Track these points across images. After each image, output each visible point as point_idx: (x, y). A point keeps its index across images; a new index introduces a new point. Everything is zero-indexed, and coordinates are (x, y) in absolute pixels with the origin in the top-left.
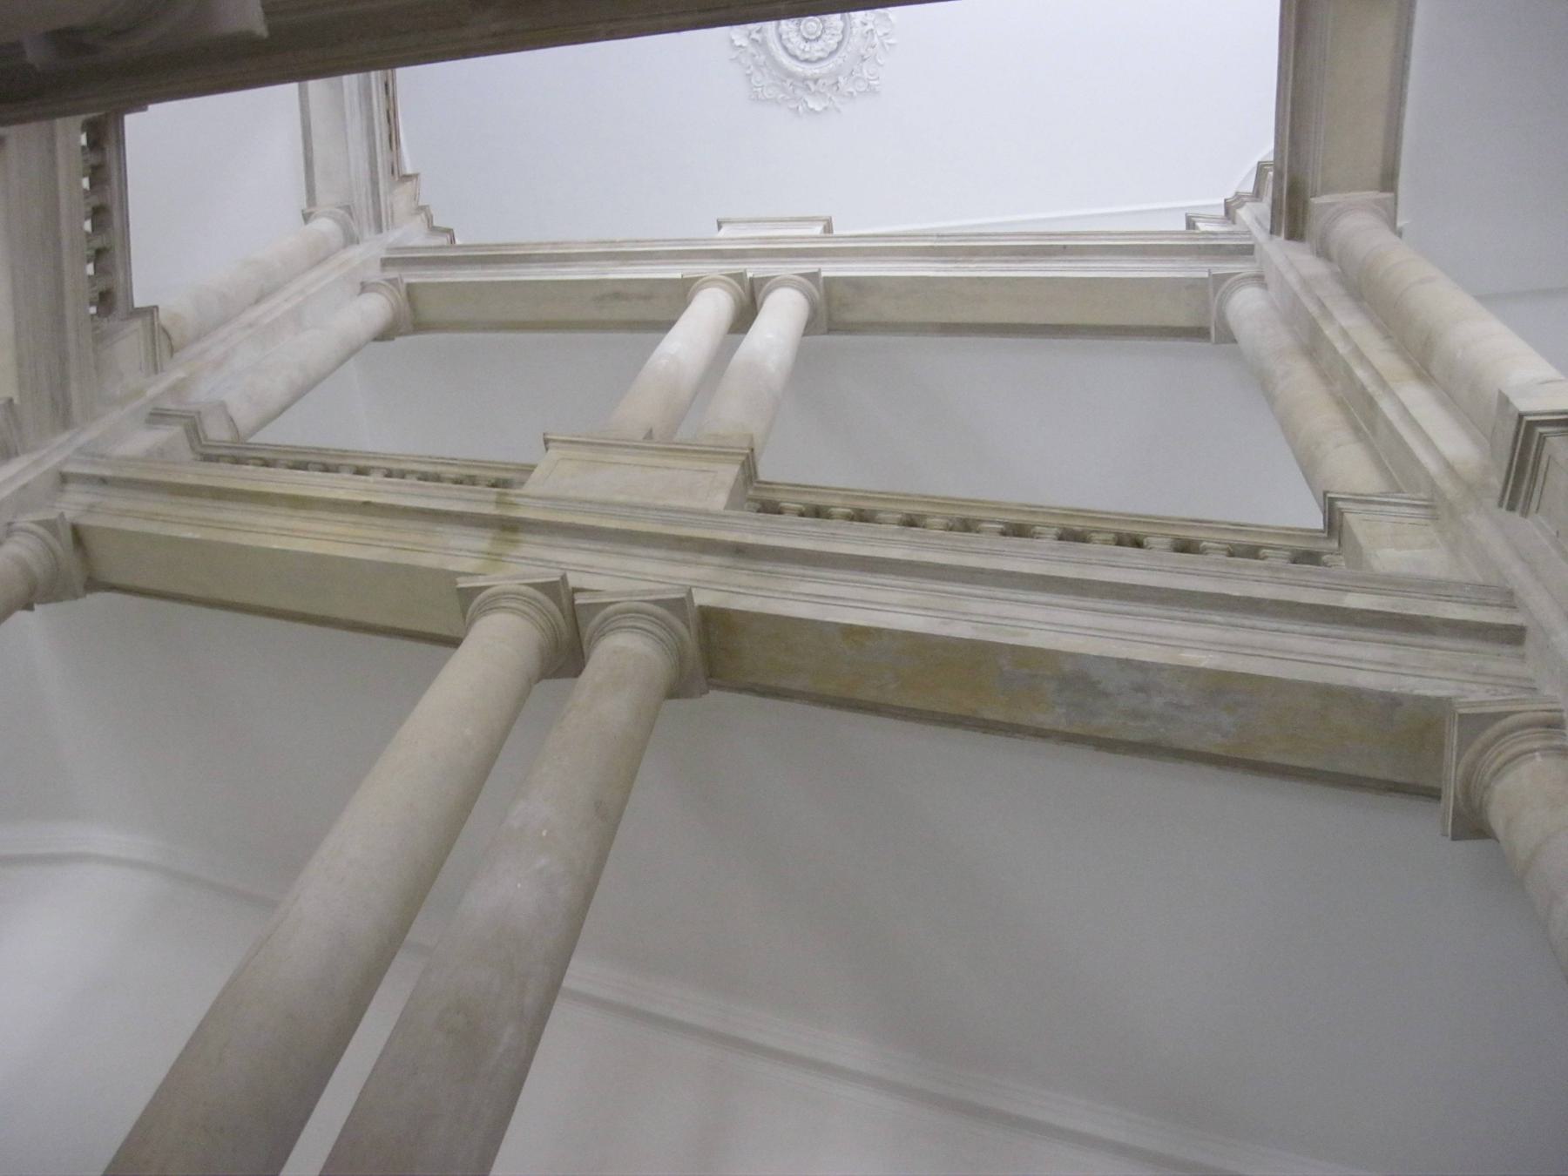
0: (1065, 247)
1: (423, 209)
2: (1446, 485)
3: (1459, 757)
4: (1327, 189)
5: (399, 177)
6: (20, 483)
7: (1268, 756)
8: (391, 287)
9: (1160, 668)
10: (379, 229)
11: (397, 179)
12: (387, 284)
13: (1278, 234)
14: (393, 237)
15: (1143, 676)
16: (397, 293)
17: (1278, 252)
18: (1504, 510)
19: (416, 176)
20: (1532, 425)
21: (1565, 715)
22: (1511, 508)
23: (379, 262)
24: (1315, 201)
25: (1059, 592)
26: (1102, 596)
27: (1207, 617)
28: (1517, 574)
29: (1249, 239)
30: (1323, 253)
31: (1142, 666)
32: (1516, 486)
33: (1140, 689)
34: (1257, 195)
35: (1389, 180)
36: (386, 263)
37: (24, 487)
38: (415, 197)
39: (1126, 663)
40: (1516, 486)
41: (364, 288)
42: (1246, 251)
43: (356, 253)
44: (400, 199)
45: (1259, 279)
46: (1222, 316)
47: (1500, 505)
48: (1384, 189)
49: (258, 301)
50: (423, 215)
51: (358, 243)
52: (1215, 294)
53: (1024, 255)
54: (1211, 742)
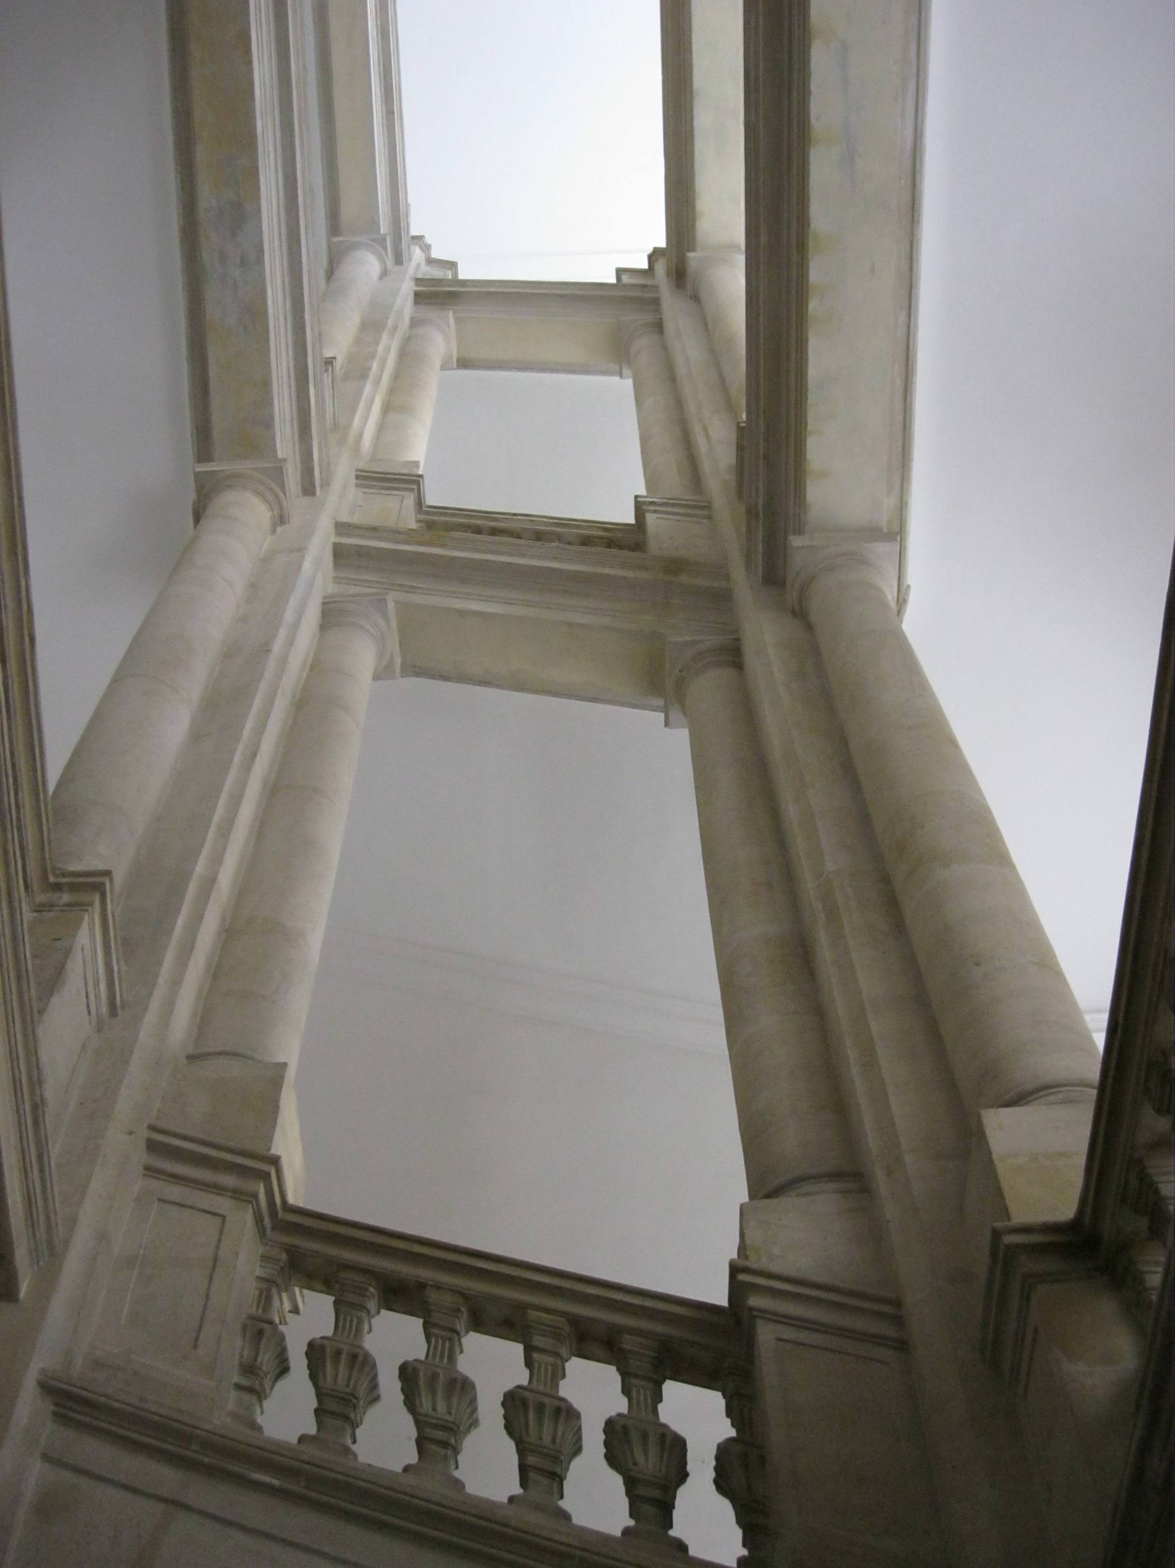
0: (393, 113)
2: (351, 438)
3: (254, 469)
4: (459, 321)
7: (212, 352)
9: (262, 273)
13: (417, 285)
15: (253, 261)
17: (407, 288)
18: (355, 473)
20: (418, 483)
21: (287, 525)
22: (357, 477)
24: (451, 312)
25: (286, 194)
26: (288, 223)
27: (288, 299)
28: (336, 486)
29: (406, 262)
30: (415, 323)
31: (260, 260)
32: (375, 479)
33: (243, 262)
34: (431, 261)
35: (464, 363)
39: (260, 251)
40: (375, 479)
42: (399, 260)
45: (384, 273)
46: (355, 246)
47: (357, 470)
48: (458, 360)
52: (373, 240)
53: (385, 77)
54: (212, 311)
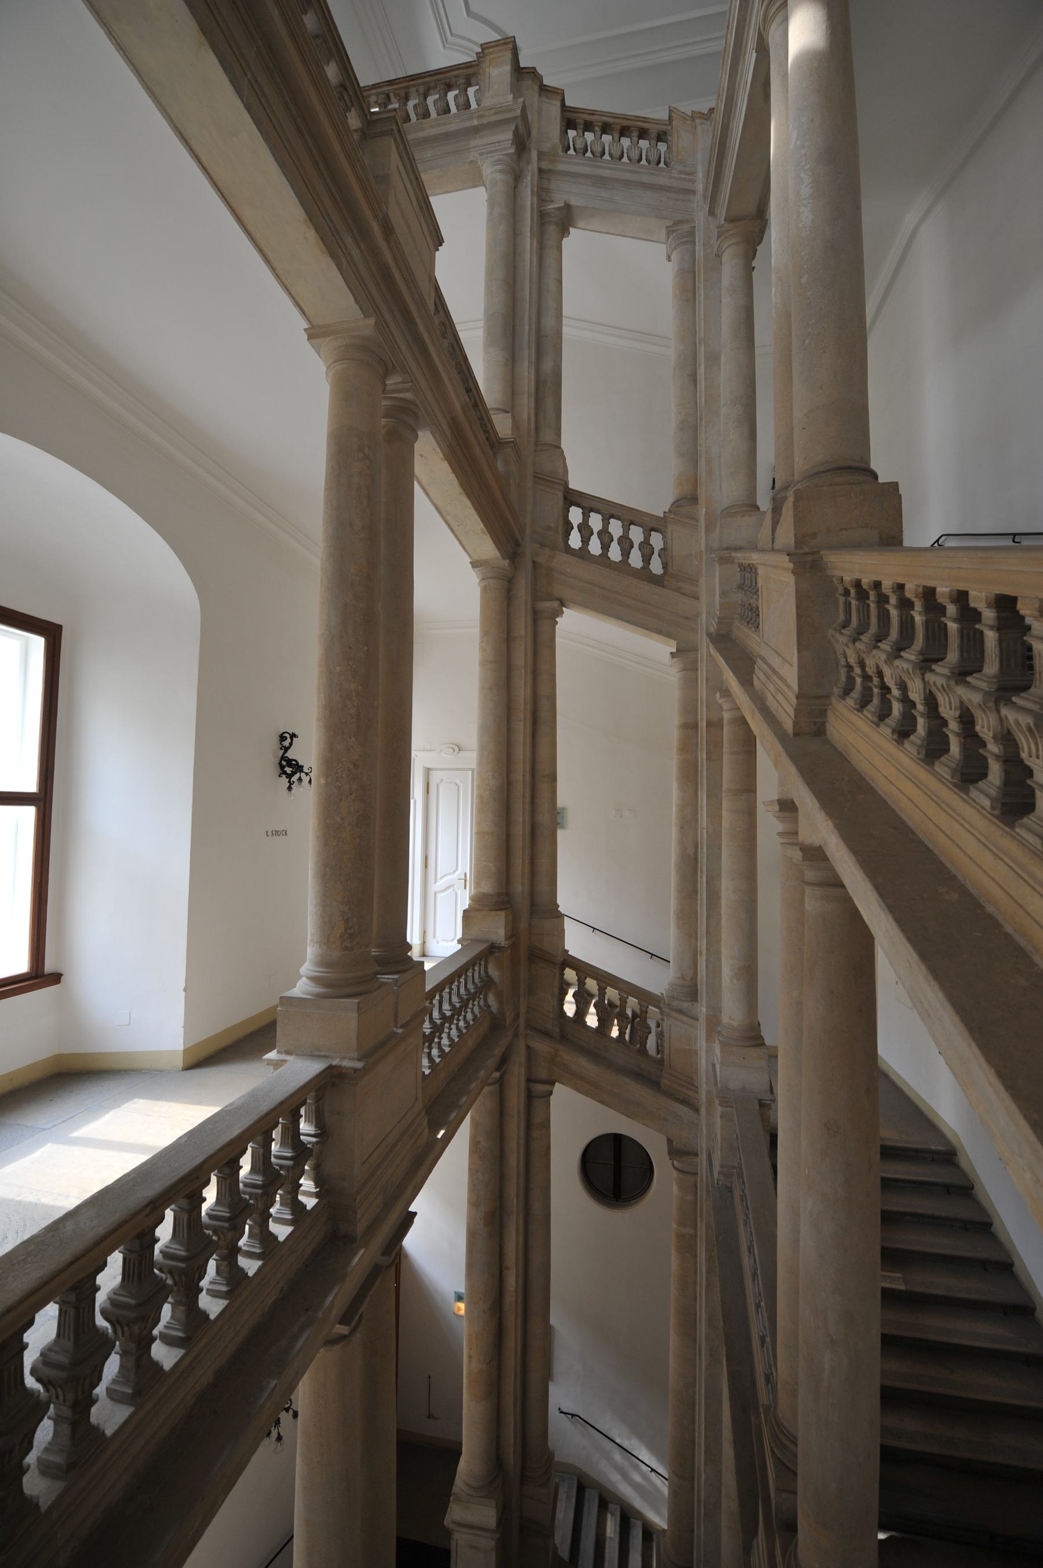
1: (693, 118)
5: (669, 125)
6: (705, 681)
8: (722, 238)
10: (693, 192)
11: (670, 127)
12: (719, 241)
14: (700, 187)
16: (731, 232)
19: (670, 111)
23: (710, 218)
36: (712, 212)
37: (707, 679)
38: (684, 117)
41: (719, 256)
43: (699, 236)
44: (681, 138)
49: (696, 385)
50: (698, 121)
51: (694, 227)
